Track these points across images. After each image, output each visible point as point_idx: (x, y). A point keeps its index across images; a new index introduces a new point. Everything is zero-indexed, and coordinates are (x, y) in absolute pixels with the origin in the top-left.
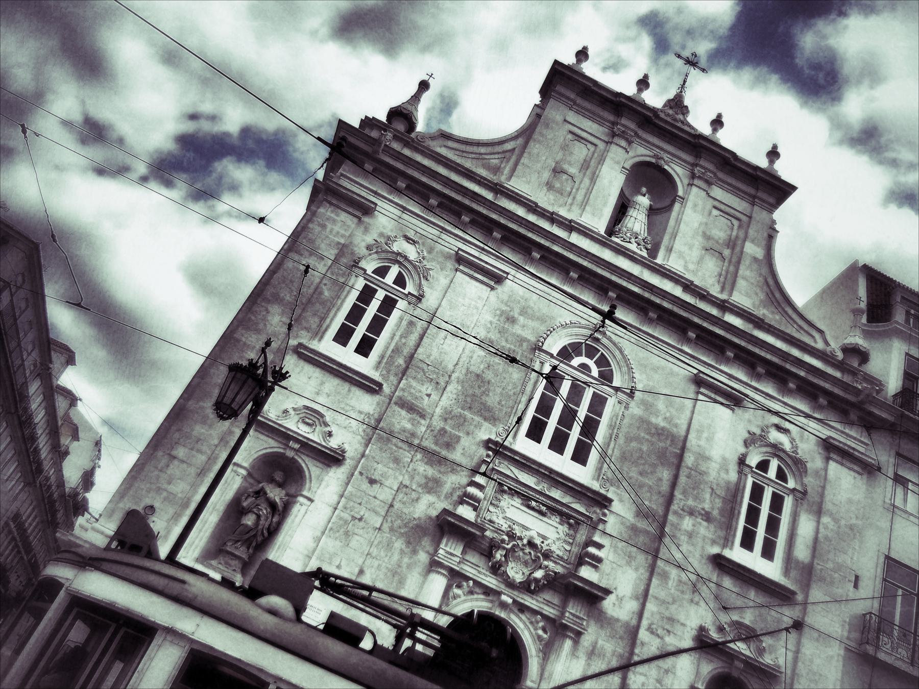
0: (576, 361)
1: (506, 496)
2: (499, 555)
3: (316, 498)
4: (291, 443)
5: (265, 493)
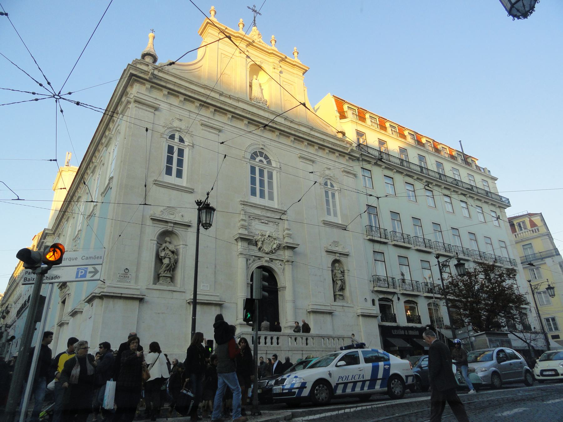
0: (258, 159)
1: (253, 221)
2: (259, 244)
3: (187, 244)
4: (170, 224)
5: (168, 248)
